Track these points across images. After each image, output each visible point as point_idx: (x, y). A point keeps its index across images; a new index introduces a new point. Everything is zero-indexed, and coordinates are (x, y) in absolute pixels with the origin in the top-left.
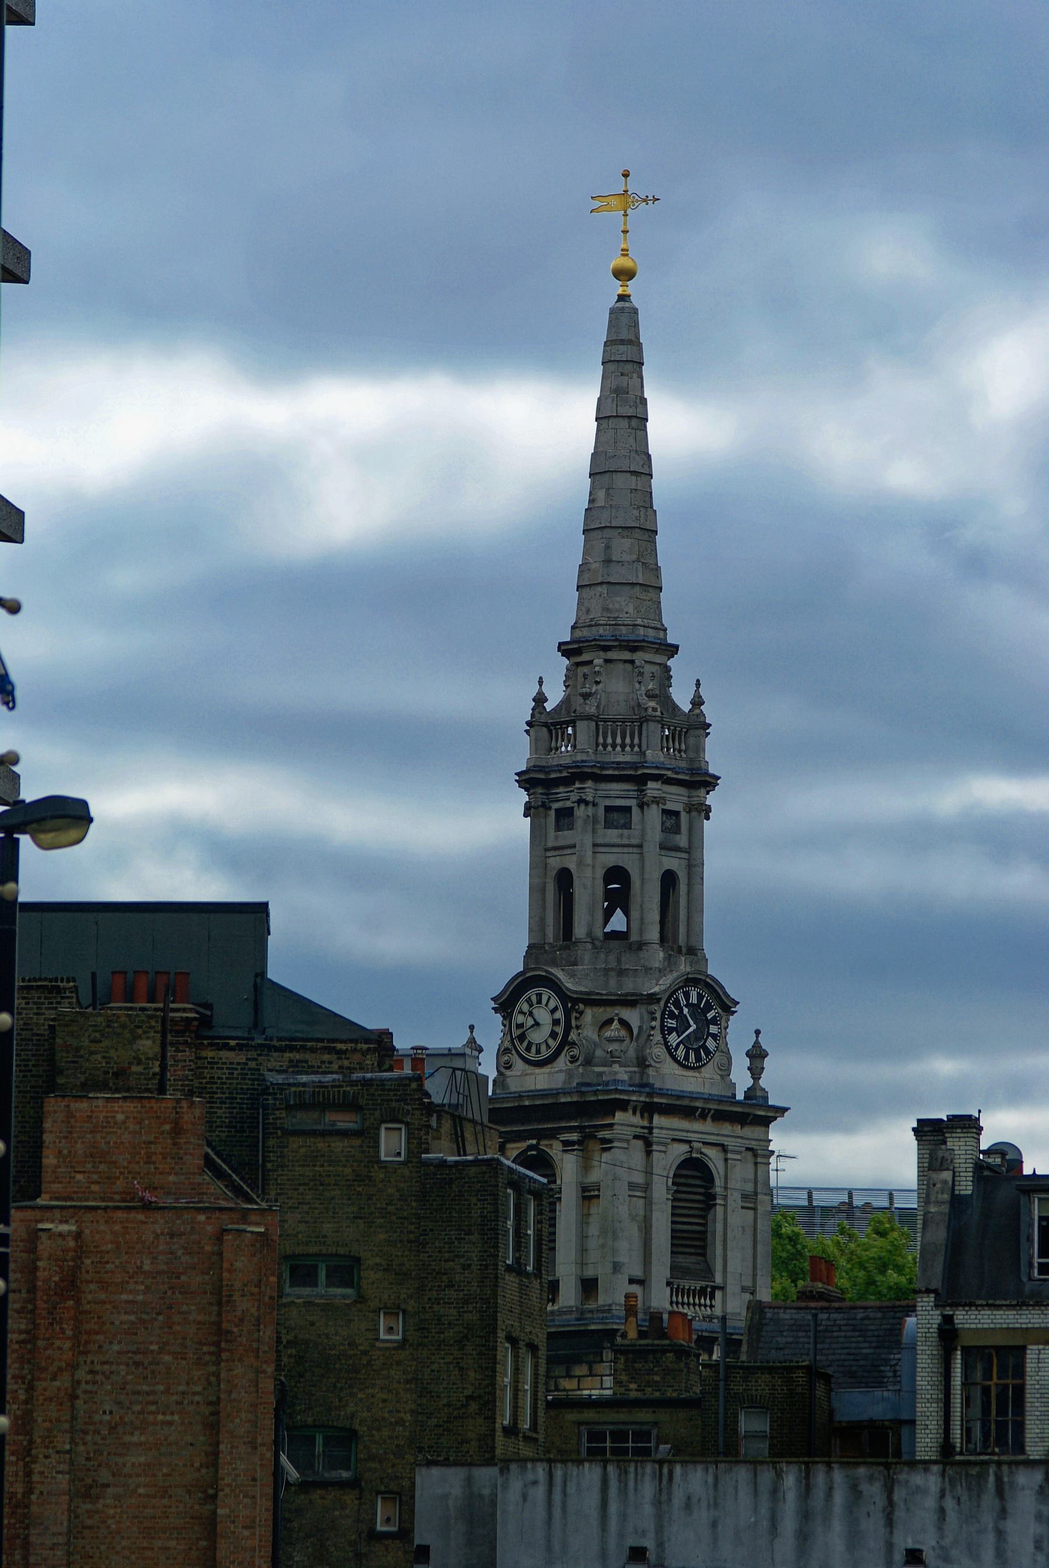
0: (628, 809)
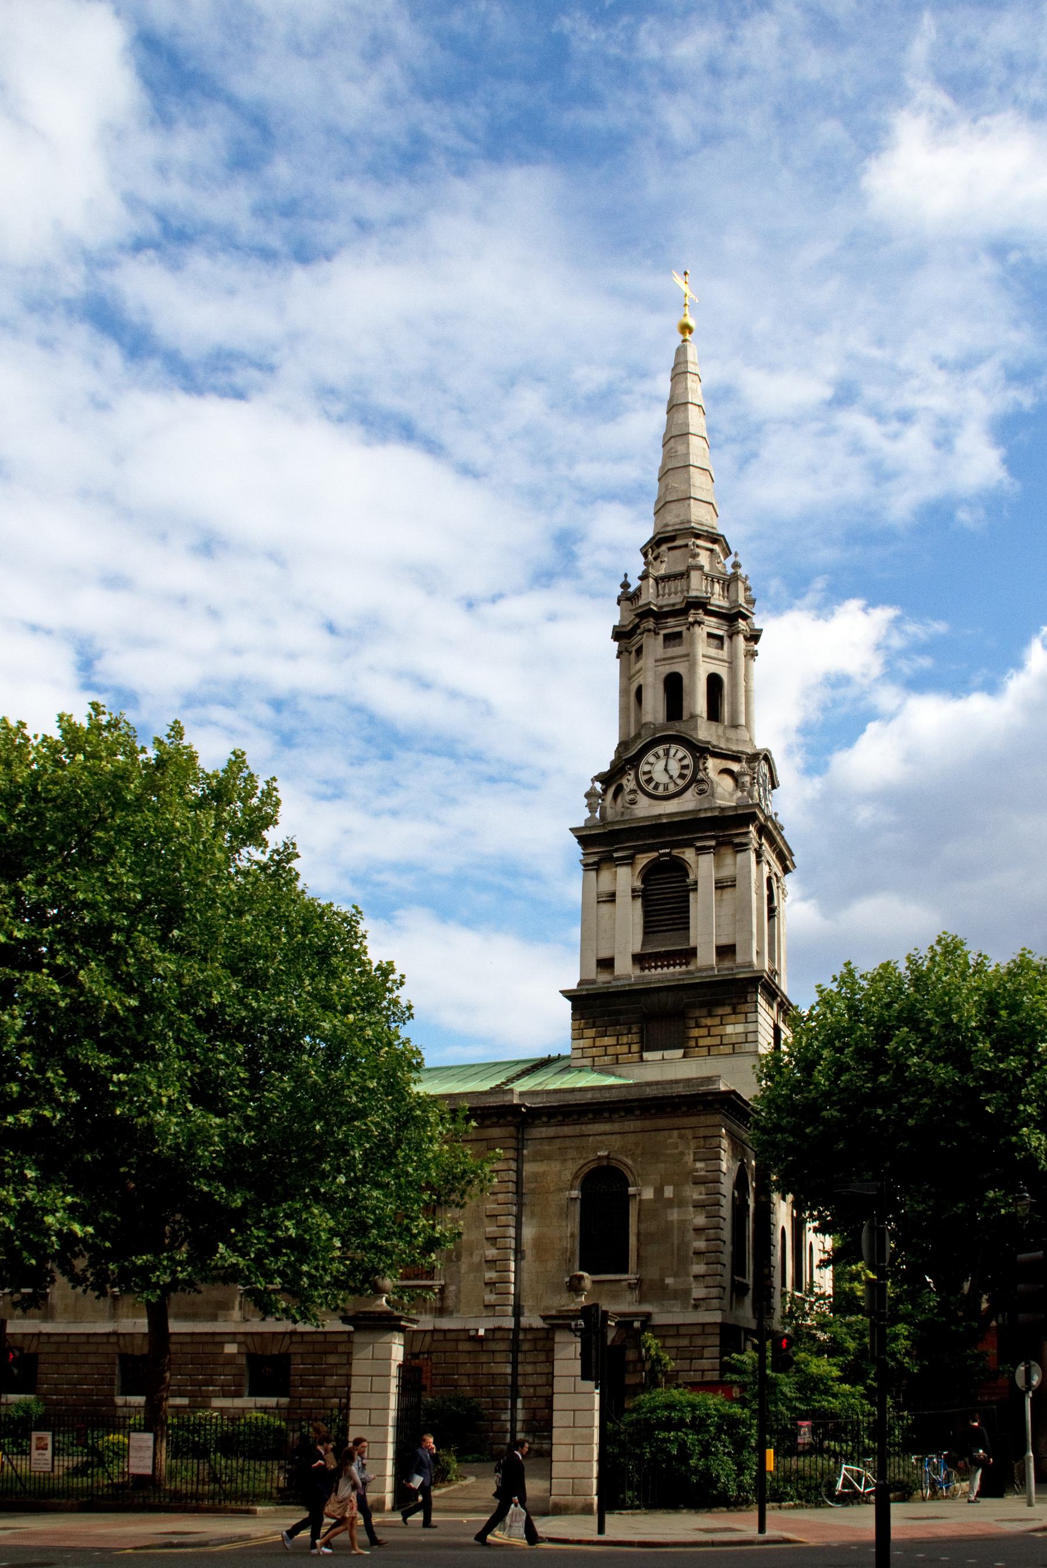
0: (720, 638)
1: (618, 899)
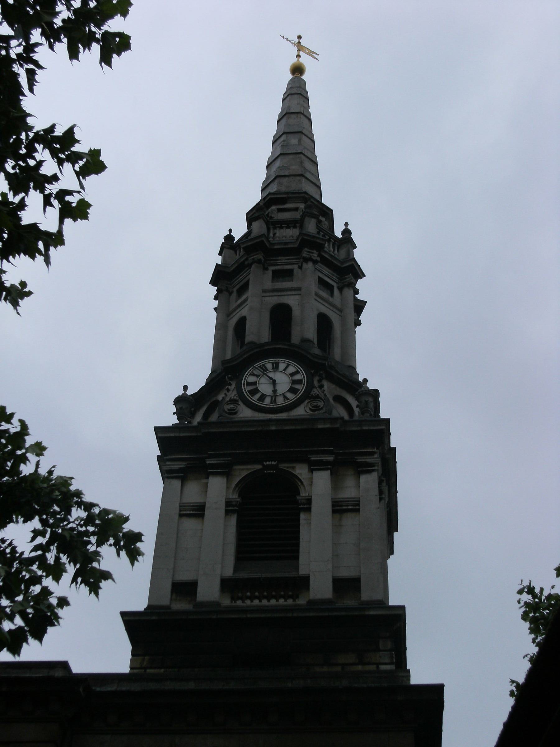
1: (207, 512)
